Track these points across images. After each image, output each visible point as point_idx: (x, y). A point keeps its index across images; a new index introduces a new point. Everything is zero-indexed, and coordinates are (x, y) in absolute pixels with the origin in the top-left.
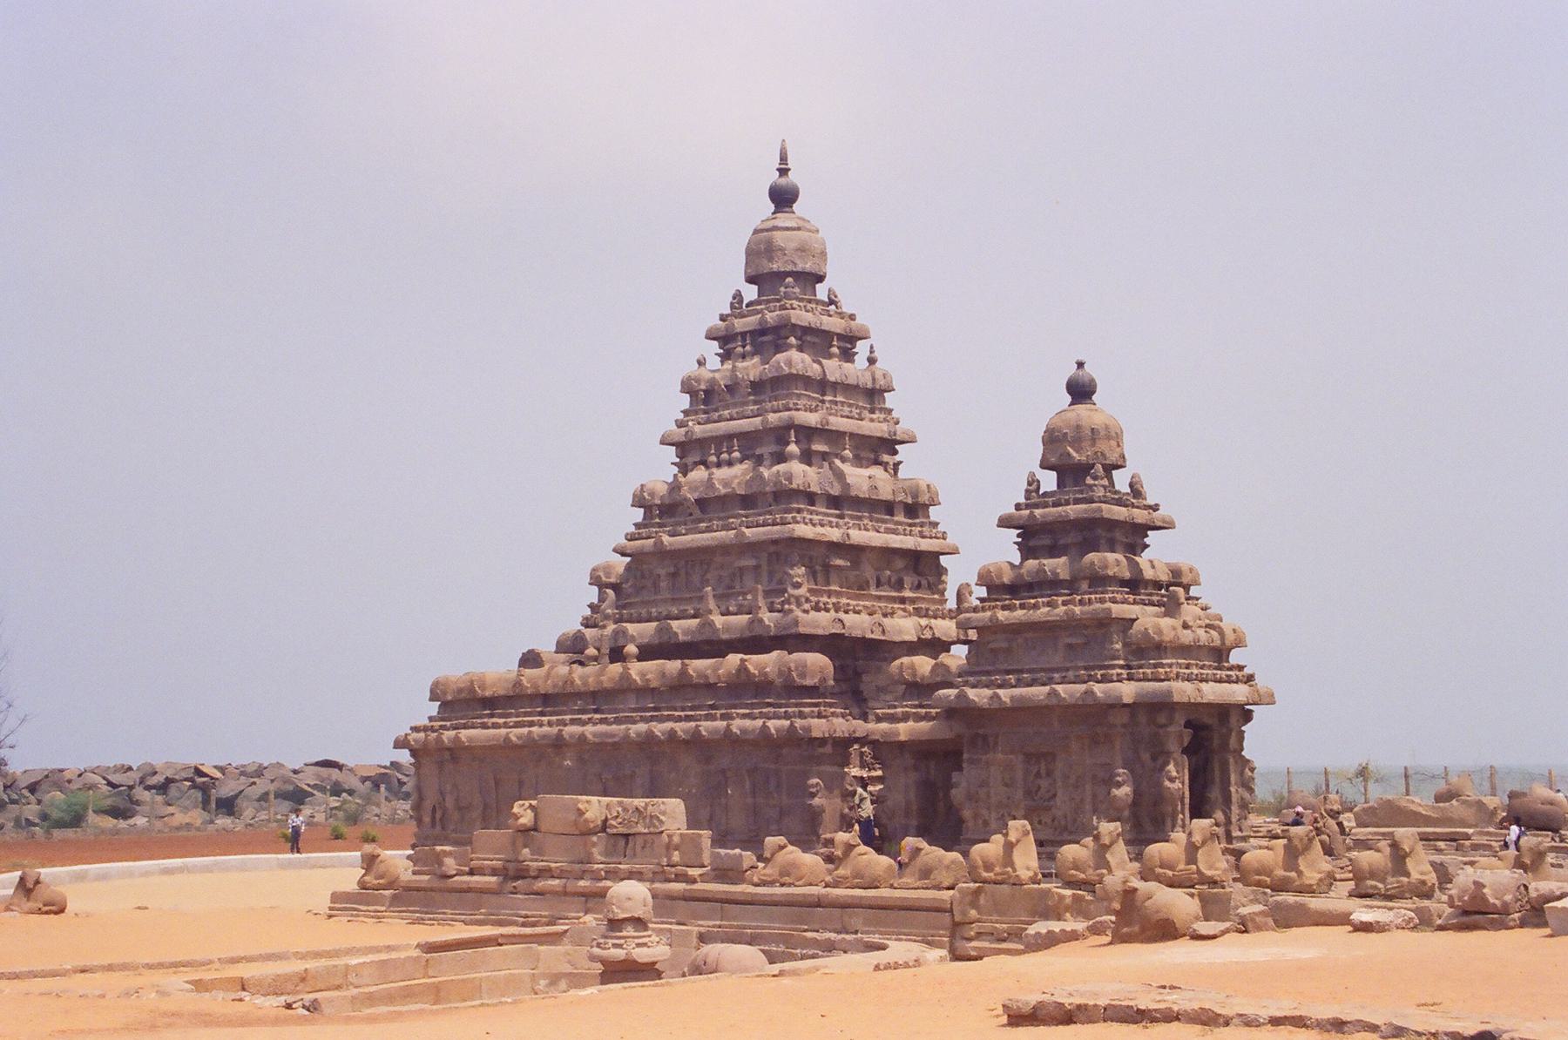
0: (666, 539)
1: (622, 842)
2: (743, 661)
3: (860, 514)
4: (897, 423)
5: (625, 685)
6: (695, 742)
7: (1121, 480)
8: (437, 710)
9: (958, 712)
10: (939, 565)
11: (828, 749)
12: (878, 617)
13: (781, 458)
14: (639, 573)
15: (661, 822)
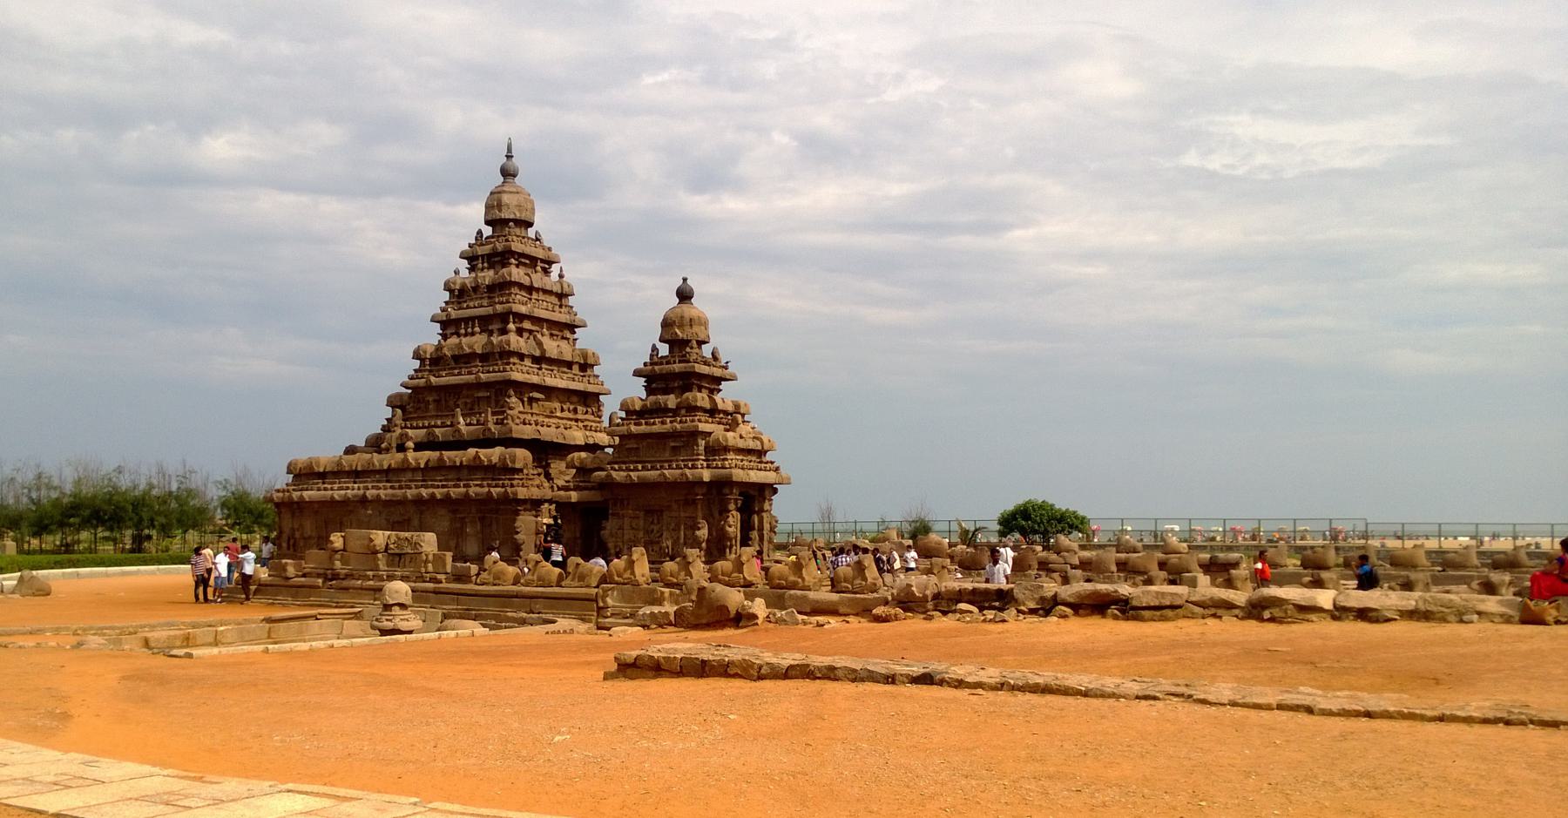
0: (433, 379)
1: (398, 559)
2: (477, 452)
4: (576, 315)
5: (406, 466)
6: (447, 500)
7: (706, 351)
9: (607, 485)
12: (562, 430)
13: (504, 331)
14: (416, 400)
15: (421, 546)
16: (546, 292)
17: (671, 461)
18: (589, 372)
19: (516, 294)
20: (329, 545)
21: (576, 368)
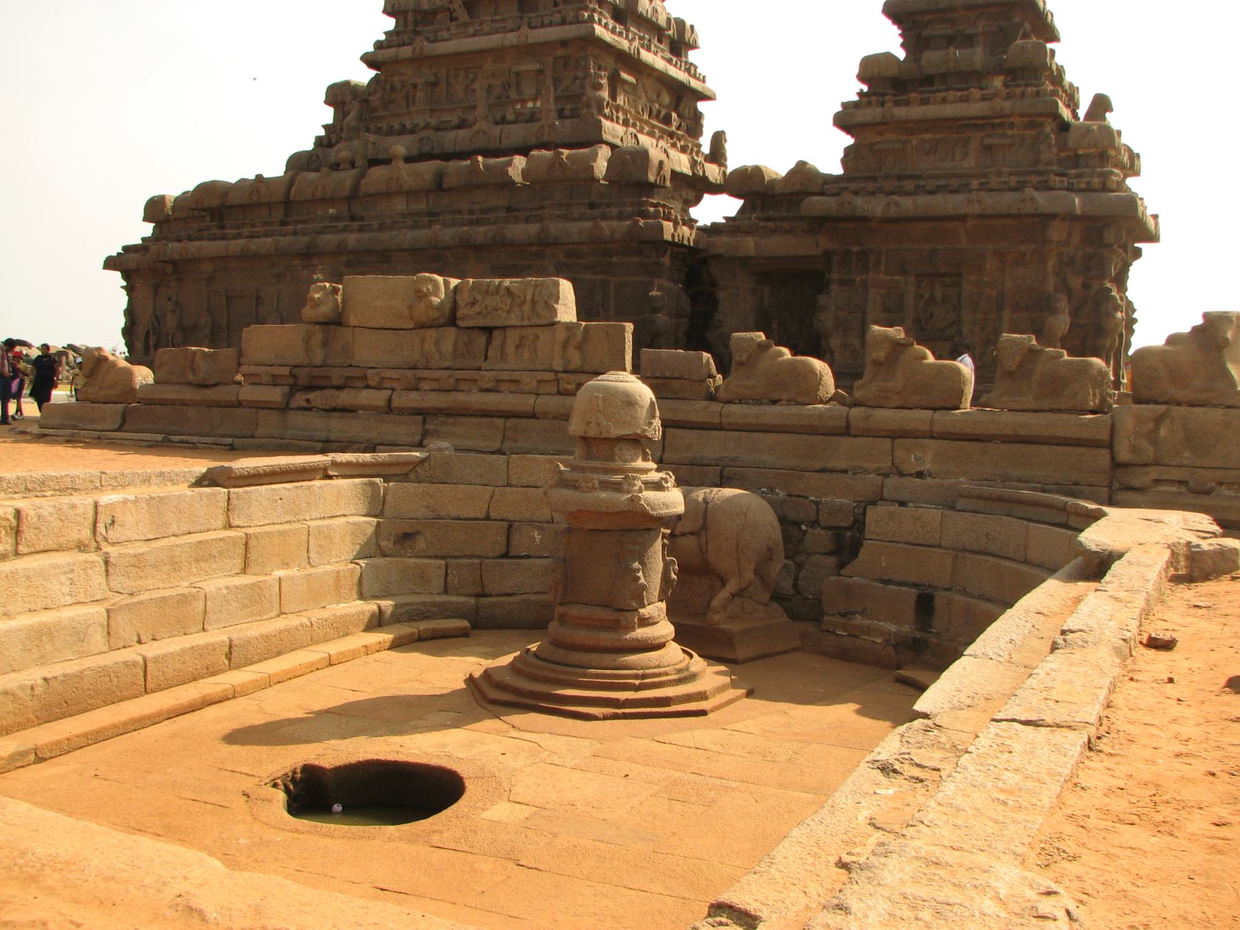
1: (481, 340)
8: (151, 231)
10: (696, 109)
11: (666, 260)
14: (388, 86)
17: (986, 176)
20: (308, 312)
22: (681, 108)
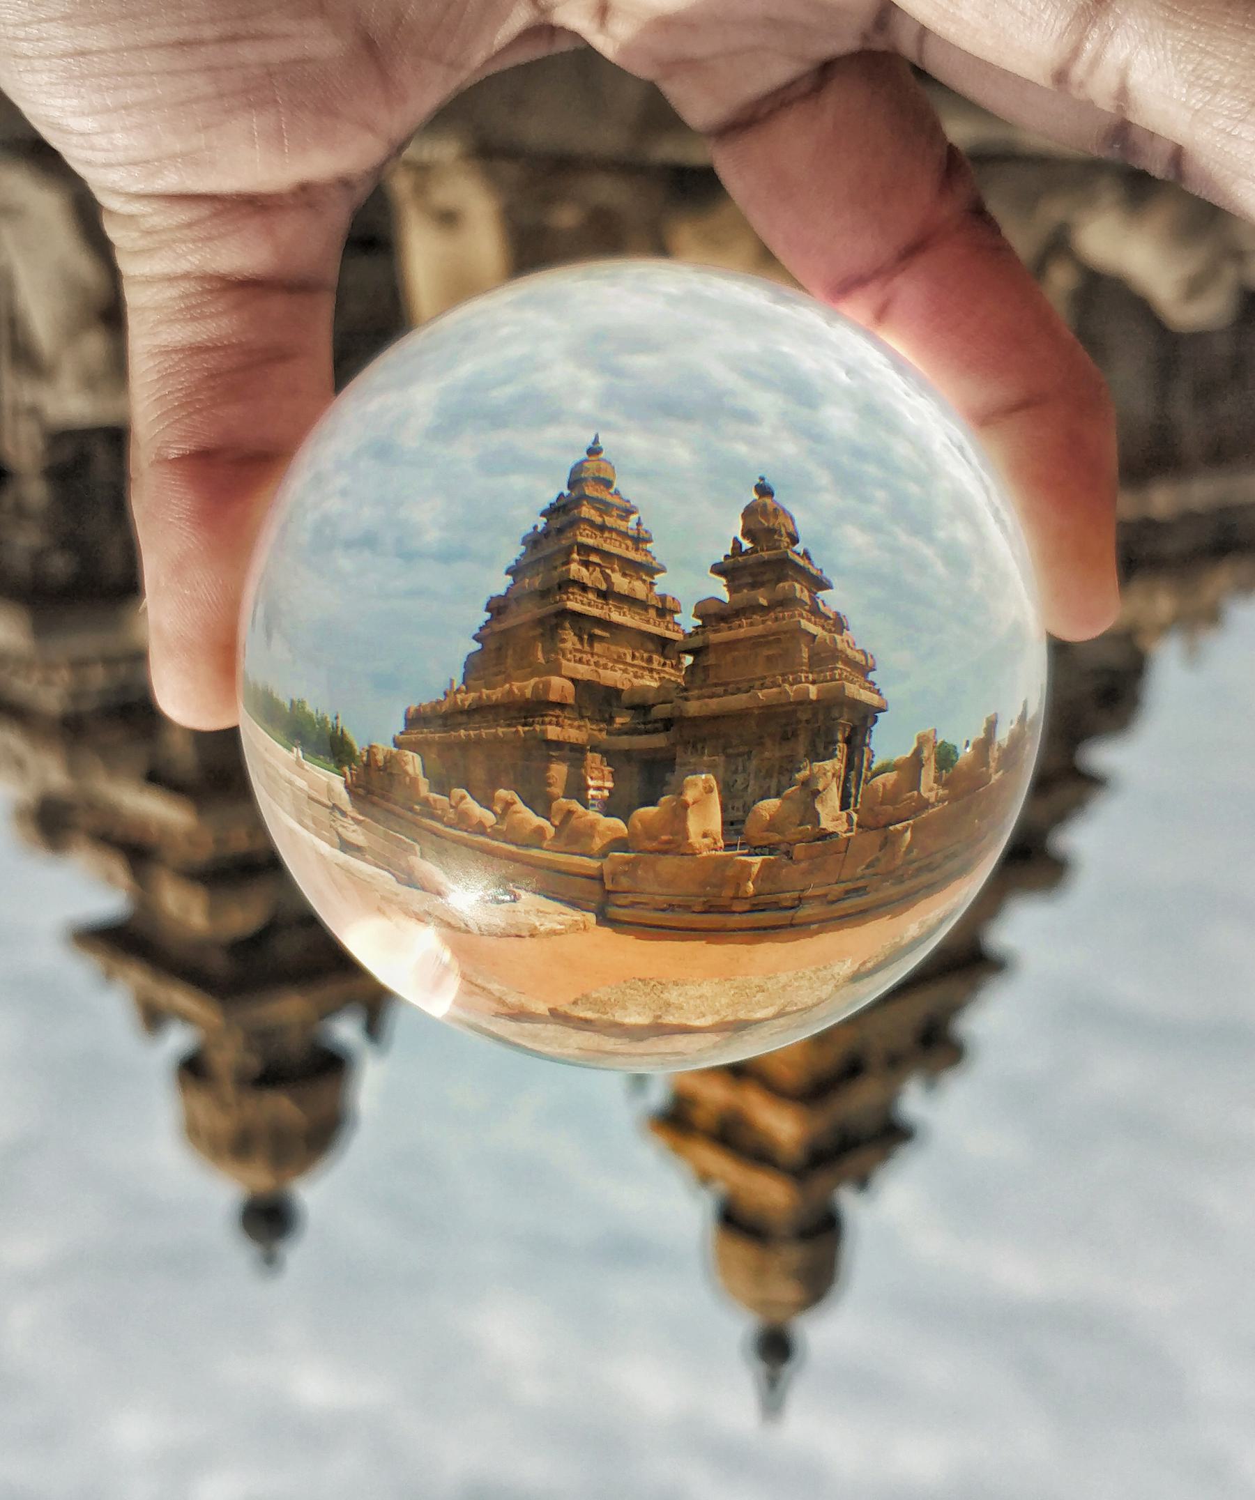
3: (621, 606)
16: (620, 533)
17: (765, 677)
18: (668, 618)
19: (585, 530)
21: (652, 613)
22: (666, 652)
